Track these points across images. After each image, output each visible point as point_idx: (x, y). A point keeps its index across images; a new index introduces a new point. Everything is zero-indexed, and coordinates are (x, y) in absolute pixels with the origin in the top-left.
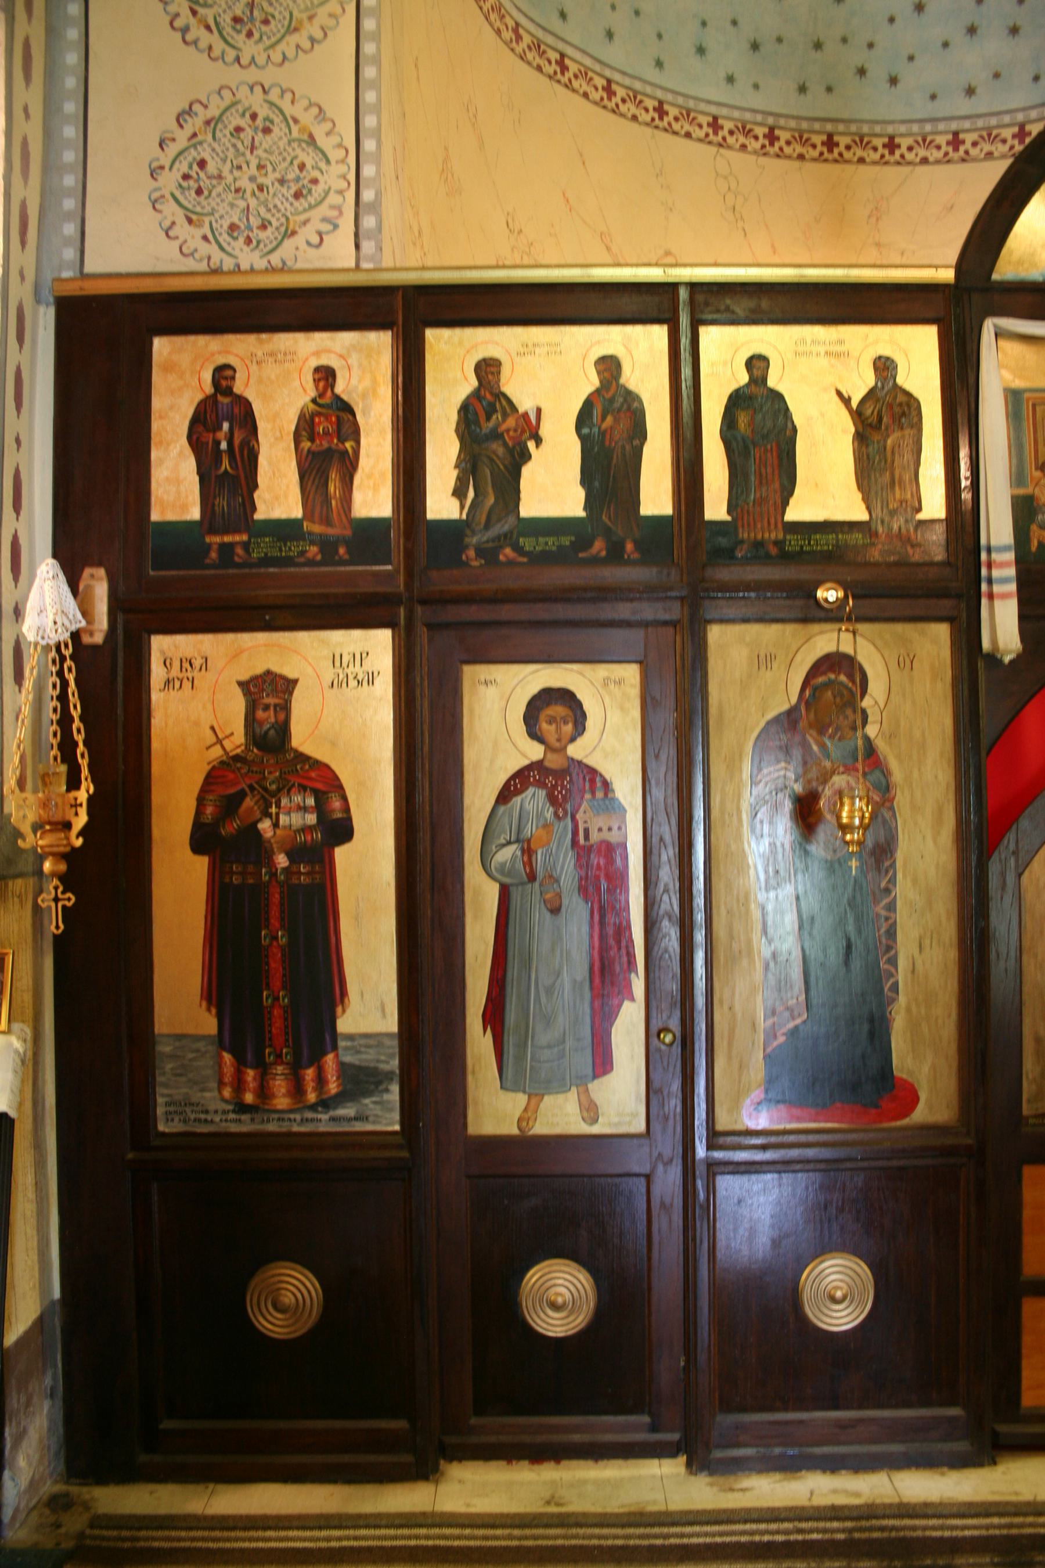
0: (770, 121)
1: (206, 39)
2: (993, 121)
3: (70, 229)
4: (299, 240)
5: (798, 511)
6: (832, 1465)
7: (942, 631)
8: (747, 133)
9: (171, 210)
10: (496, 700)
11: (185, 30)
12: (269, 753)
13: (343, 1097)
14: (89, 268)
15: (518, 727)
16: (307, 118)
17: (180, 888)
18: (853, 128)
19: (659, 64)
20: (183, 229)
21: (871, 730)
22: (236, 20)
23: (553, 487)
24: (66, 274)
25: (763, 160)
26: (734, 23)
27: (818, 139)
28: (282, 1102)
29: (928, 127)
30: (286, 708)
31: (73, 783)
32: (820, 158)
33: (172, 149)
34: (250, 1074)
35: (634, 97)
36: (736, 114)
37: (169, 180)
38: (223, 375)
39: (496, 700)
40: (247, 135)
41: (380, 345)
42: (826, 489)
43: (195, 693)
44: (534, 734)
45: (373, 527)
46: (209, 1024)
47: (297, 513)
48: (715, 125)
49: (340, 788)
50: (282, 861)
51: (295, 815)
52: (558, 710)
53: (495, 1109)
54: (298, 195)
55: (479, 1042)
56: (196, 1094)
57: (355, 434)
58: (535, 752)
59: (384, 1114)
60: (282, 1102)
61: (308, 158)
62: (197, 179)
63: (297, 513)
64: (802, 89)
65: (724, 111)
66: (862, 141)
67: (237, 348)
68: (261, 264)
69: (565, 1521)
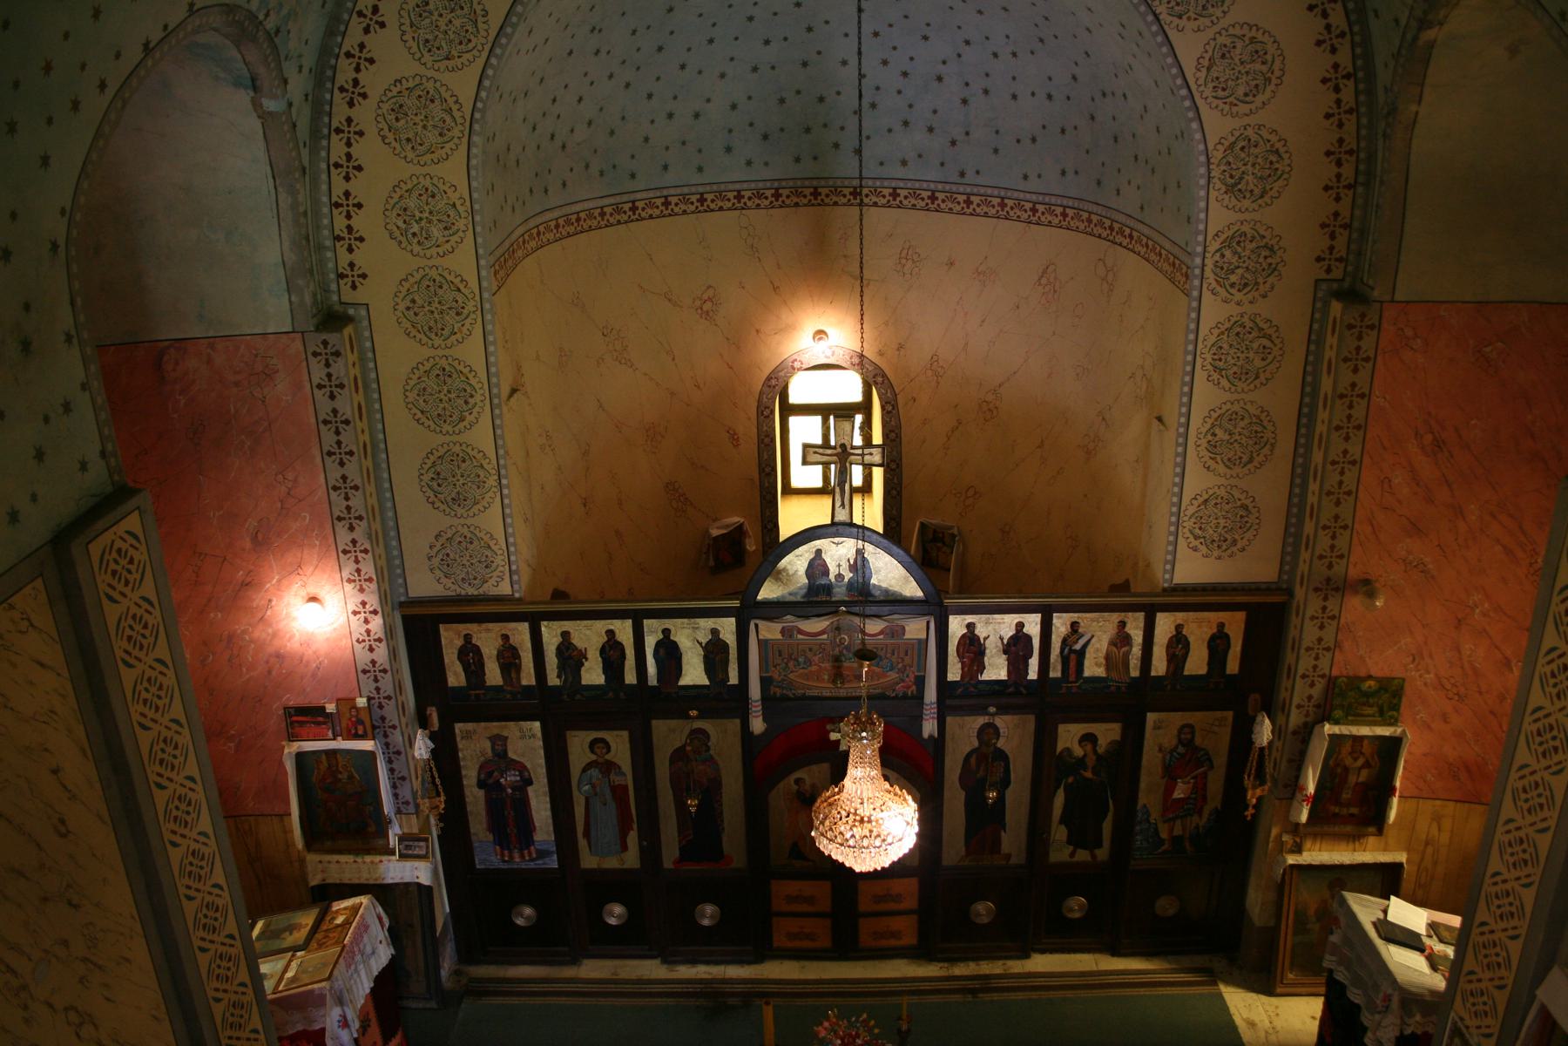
0: (776, 184)
1: (442, 507)
2: (917, 185)
3: (400, 581)
5: (682, 682)
6: (707, 963)
7: (738, 721)
8: (760, 196)
9: (437, 572)
10: (579, 744)
12: (500, 757)
14: (412, 594)
16: (486, 538)
17: (475, 797)
18: (831, 183)
19: (700, 169)
20: (444, 580)
23: (593, 675)
24: (403, 599)
25: (771, 211)
26: (751, 125)
27: (807, 192)
29: (878, 183)
31: (438, 795)
32: (809, 204)
35: (684, 198)
36: (753, 185)
37: (436, 561)
41: (524, 627)
42: (694, 673)
43: (473, 743)
44: (592, 752)
45: (529, 687)
46: (491, 838)
48: (739, 197)
49: (525, 767)
51: (512, 777)
53: (589, 861)
55: (582, 842)
56: (487, 855)
57: (519, 657)
58: (594, 757)
59: (553, 863)
61: (489, 553)
62: (446, 561)
64: (798, 160)
65: (745, 186)
66: (836, 191)
67: (472, 628)
69: (615, 982)
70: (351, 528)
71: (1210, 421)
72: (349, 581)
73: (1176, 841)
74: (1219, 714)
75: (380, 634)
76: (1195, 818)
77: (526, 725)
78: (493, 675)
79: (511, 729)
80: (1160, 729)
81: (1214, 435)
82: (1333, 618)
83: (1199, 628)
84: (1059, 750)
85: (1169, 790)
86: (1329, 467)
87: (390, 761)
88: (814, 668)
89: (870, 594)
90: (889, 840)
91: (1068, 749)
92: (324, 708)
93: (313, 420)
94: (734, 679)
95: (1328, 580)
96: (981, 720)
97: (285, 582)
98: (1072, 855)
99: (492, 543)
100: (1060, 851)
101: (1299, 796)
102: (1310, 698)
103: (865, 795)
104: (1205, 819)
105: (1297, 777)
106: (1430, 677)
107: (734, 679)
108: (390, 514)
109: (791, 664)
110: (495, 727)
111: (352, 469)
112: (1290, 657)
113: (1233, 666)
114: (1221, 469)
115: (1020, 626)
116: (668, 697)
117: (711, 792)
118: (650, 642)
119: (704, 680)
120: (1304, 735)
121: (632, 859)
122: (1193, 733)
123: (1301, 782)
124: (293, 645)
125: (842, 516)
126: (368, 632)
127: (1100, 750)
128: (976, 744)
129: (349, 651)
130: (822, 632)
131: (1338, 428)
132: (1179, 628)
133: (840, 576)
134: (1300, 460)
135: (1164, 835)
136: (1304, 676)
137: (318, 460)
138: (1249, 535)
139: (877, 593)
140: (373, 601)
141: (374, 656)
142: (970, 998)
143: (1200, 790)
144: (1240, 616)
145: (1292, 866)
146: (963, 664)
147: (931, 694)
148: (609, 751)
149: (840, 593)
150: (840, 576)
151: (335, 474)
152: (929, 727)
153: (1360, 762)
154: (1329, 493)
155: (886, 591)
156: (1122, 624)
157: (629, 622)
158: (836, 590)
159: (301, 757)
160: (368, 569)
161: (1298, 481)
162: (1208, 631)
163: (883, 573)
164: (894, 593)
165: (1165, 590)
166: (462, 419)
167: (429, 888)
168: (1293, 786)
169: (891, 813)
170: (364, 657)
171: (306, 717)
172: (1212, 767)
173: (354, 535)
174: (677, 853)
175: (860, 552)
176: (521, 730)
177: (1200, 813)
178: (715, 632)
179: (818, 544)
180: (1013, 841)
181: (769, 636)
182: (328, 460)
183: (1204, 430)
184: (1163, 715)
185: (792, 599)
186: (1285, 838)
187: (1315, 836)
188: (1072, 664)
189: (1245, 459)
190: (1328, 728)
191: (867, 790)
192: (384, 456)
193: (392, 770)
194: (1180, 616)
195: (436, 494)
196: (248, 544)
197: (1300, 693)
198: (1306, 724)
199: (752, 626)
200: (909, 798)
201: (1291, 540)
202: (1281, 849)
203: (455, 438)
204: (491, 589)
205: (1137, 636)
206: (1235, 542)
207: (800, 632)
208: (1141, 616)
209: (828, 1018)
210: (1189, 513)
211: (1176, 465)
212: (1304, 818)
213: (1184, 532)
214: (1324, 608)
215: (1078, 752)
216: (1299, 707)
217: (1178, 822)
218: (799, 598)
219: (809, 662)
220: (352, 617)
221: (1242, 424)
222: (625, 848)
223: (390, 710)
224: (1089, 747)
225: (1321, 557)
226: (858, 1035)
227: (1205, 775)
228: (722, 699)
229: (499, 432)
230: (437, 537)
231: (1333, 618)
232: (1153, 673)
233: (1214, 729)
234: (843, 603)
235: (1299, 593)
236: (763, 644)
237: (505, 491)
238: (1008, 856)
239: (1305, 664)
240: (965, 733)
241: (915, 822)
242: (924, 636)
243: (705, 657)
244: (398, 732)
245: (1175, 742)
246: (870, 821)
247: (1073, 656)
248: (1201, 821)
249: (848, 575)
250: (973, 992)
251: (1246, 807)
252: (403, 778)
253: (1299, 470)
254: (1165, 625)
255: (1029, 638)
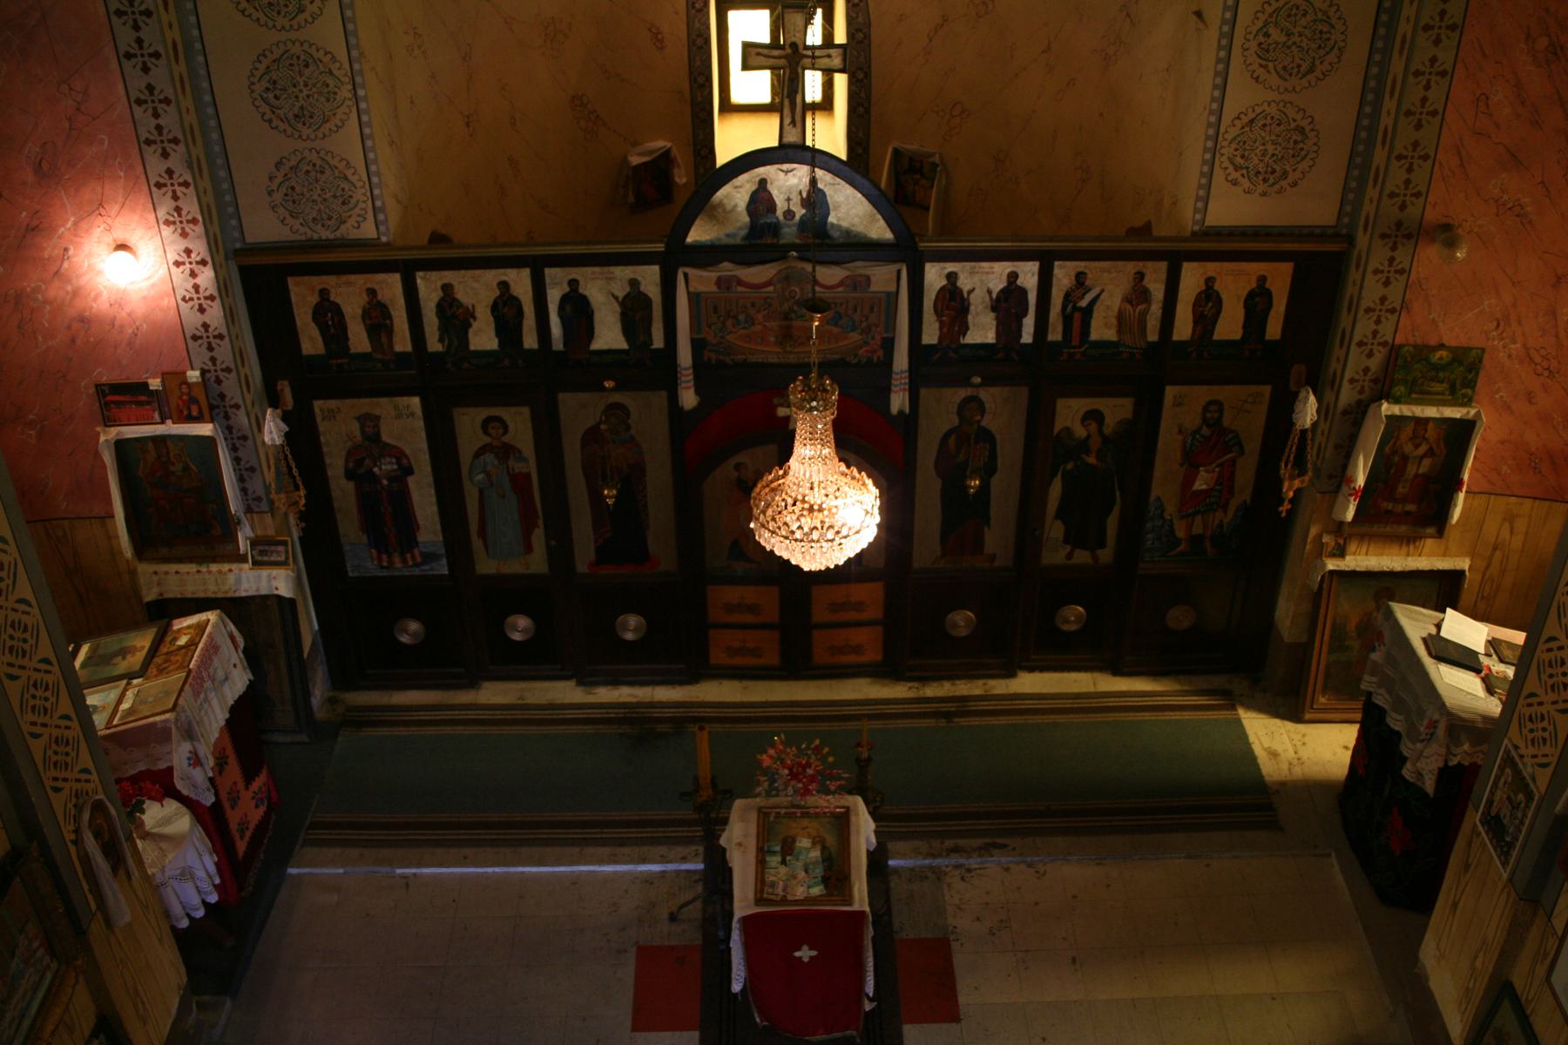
1: (282, 126)
4: (348, 225)
5: (597, 345)
6: (631, 684)
7: (664, 394)
9: (281, 210)
10: (469, 424)
11: (270, 121)
12: (372, 441)
13: (424, 563)
14: (249, 239)
15: (479, 431)
17: (343, 491)
20: (289, 220)
21: (633, 431)
22: (296, 116)
23: (483, 338)
24: (238, 245)
28: (398, 565)
30: (377, 426)
31: (297, 488)
33: (277, 181)
34: (384, 556)
37: (278, 197)
38: (324, 293)
39: (469, 424)
40: (313, 174)
42: (609, 335)
43: (338, 424)
44: (486, 432)
45: (402, 356)
46: (365, 538)
47: (369, 349)
50: (385, 482)
51: (388, 466)
52: (497, 424)
53: (486, 566)
54: (344, 203)
55: (477, 543)
56: (361, 560)
57: (390, 318)
58: (488, 440)
59: (442, 568)
60: (398, 565)
61: (346, 186)
63: (369, 349)
67: (330, 281)
68: (332, 237)
70: (165, 155)
71: (1263, 17)
72: (167, 223)
73: (1196, 541)
74: (1253, 388)
75: (213, 291)
76: (1219, 514)
77: (403, 401)
78: (359, 340)
79: (383, 407)
80: (1181, 407)
81: (1267, 35)
82: (1401, 272)
83: (1234, 282)
84: (1056, 430)
85: (1189, 480)
86: (1411, 79)
87: (234, 449)
88: (758, 328)
89: (829, 237)
90: (844, 533)
91: (1068, 429)
92: (146, 385)
93: (102, 11)
94: (658, 342)
95: (1399, 224)
96: (963, 393)
97: (84, 225)
98: (1069, 556)
99: (349, 173)
100: (1056, 552)
101: (1345, 489)
102: (1366, 370)
103: (815, 479)
104: (1230, 514)
105: (1345, 467)
106: (1516, 347)
107: (658, 342)
108: (215, 136)
109: (729, 323)
110: (364, 405)
111: (159, 75)
112: (1345, 320)
113: (1274, 330)
114: (1274, 80)
115: (1013, 276)
116: (577, 365)
117: (632, 482)
118: (554, 296)
119: (620, 343)
120: (1358, 414)
121: (538, 562)
122: (1221, 411)
123: (1349, 472)
124: (102, 306)
125: (792, 137)
126: (196, 288)
127: (1107, 431)
128: (956, 422)
129: (173, 312)
130: (768, 284)
131: (1427, 28)
132: (1209, 281)
133: (789, 214)
134: (1375, 70)
135: (1180, 533)
136: (1360, 344)
137: (114, 65)
138: (1305, 165)
139: (835, 234)
140: (200, 249)
141: (206, 318)
142: (943, 723)
143: (1226, 482)
144: (1286, 268)
145: (1332, 572)
146: (941, 323)
147: (901, 361)
148: (506, 429)
149: (789, 234)
150: (789, 214)
151: (138, 82)
152: (898, 401)
153: (1423, 448)
154: (1408, 113)
155: (848, 232)
156: (1140, 276)
157: (526, 272)
158: (786, 230)
159: (121, 446)
160: (191, 207)
161: (1370, 97)
162: (1247, 285)
163: (843, 210)
164: (857, 235)
165: (1194, 234)
166: (301, 10)
167: (292, 602)
168: (1341, 476)
169: (848, 501)
170: (193, 320)
171: (123, 396)
172: (1242, 453)
173: (170, 163)
174: (592, 556)
175: (813, 181)
176: (396, 408)
177: (1225, 508)
178: (634, 283)
179: (762, 171)
180: (997, 539)
181: (701, 288)
182: (127, 64)
183: (1254, 29)
184: (1186, 389)
185: (731, 241)
186: (1326, 539)
187: (1362, 537)
188: (1076, 324)
189: (1305, 66)
190: (1386, 408)
191: (816, 472)
192: (201, 59)
193: (237, 460)
194: (1212, 268)
195: (273, 109)
196: (30, 177)
197: (1354, 365)
198: (1359, 402)
199: (680, 277)
200: (869, 482)
201: (1356, 173)
202: (1320, 552)
203: (293, 35)
204: (349, 231)
205: (1157, 290)
206: (1285, 175)
207: (740, 282)
208: (1163, 266)
209: (773, 745)
210: (1229, 137)
211: (1217, 74)
212: (1350, 515)
213: (1222, 161)
214: (1392, 260)
215: (1080, 432)
216: (1352, 381)
217: (1198, 519)
218: (738, 241)
219: (751, 321)
220: (174, 269)
221: (1303, 22)
222: (529, 549)
223: (230, 386)
224: (1093, 427)
225: (1392, 195)
226: (808, 765)
227: (1234, 461)
228: (646, 367)
229: (350, 27)
230: (278, 165)
231: (1401, 272)
232: (1175, 338)
233: (1245, 407)
234: (794, 247)
235: (1362, 240)
236: (694, 298)
237: (363, 105)
238: (993, 558)
239: (1363, 328)
240: (942, 410)
241: (876, 511)
242: (893, 289)
243: (624, 315)
244: (242, 413)
245: (1198, 421)
246: (821, 510)
247: (1077, 315)
248: (1225, 518)
249: (800, 212)
250: (948, 716)
251: (1281, 501)
252: (252, 469)
253: (1372, 84)
254: (1192, 277)
255: (1023, 292)
